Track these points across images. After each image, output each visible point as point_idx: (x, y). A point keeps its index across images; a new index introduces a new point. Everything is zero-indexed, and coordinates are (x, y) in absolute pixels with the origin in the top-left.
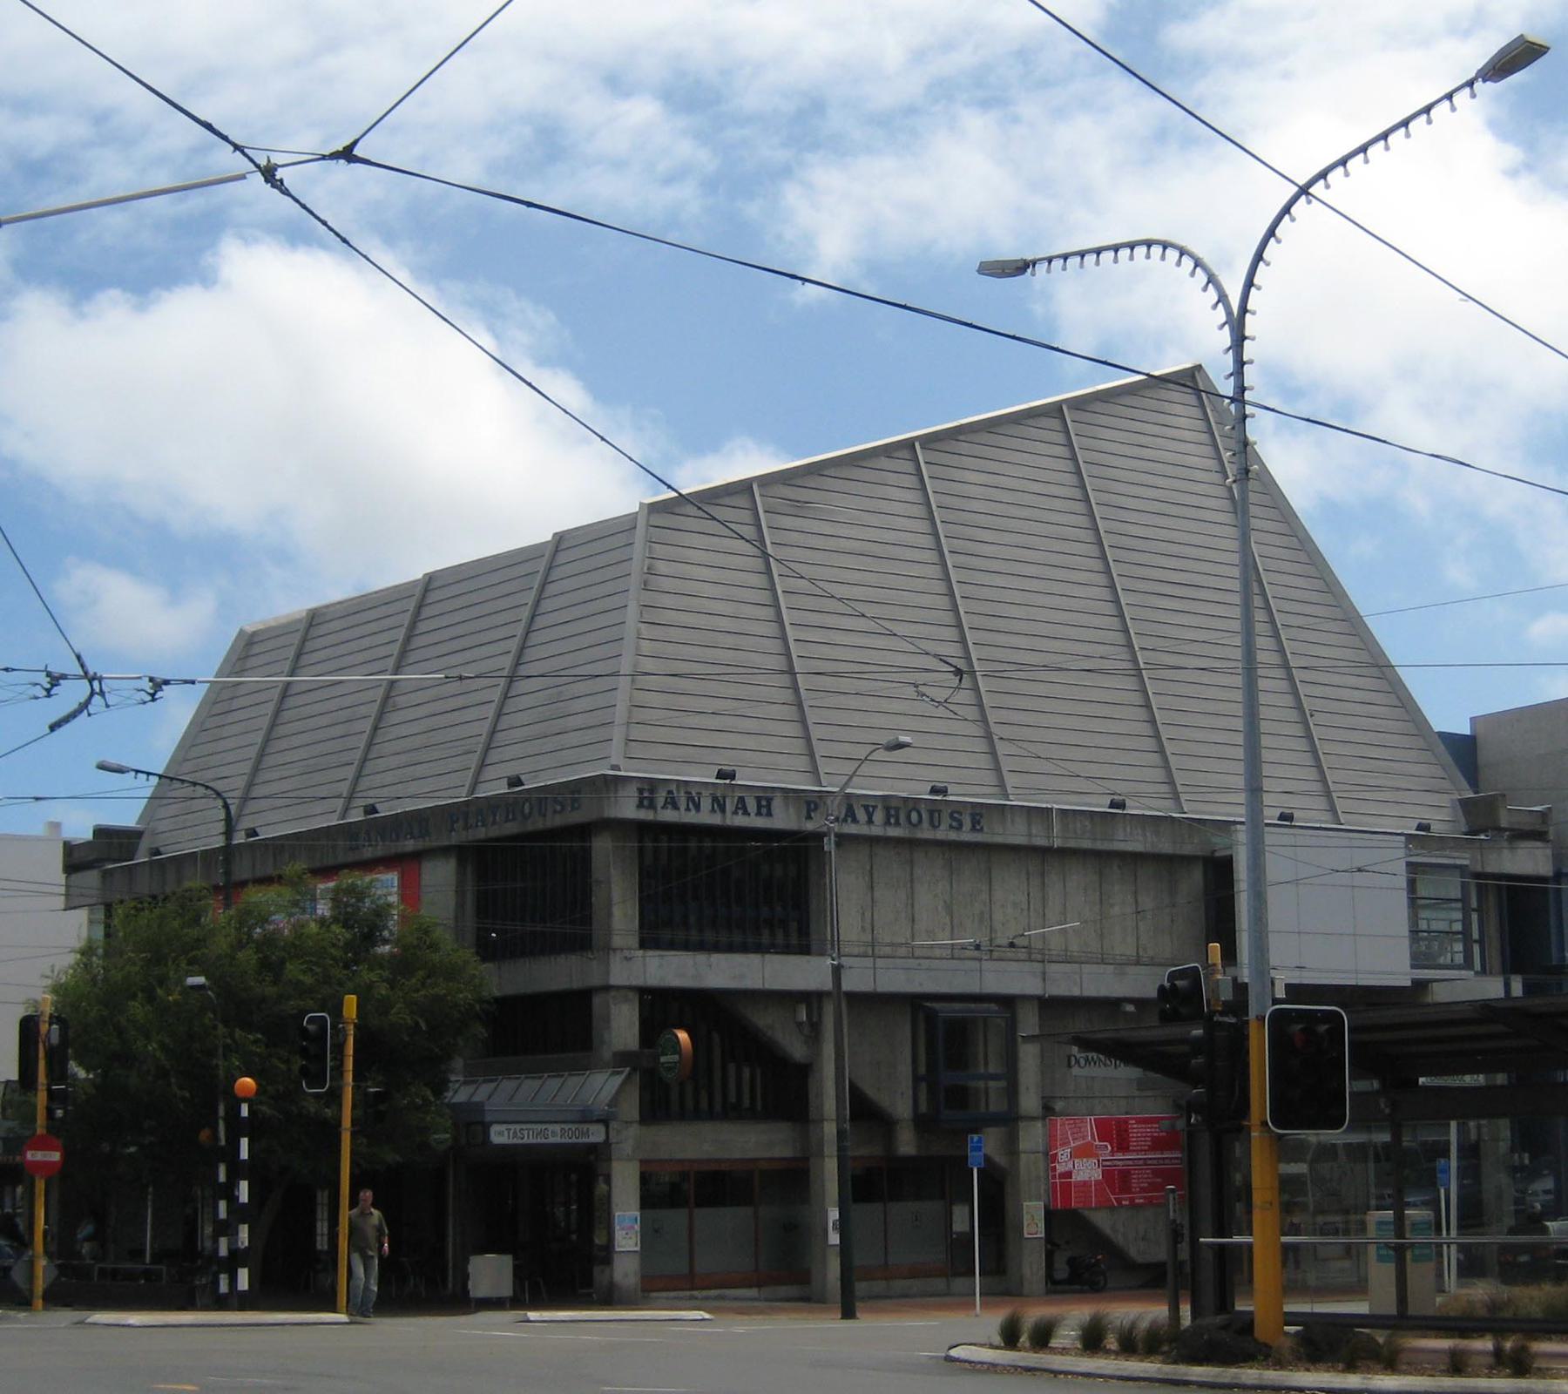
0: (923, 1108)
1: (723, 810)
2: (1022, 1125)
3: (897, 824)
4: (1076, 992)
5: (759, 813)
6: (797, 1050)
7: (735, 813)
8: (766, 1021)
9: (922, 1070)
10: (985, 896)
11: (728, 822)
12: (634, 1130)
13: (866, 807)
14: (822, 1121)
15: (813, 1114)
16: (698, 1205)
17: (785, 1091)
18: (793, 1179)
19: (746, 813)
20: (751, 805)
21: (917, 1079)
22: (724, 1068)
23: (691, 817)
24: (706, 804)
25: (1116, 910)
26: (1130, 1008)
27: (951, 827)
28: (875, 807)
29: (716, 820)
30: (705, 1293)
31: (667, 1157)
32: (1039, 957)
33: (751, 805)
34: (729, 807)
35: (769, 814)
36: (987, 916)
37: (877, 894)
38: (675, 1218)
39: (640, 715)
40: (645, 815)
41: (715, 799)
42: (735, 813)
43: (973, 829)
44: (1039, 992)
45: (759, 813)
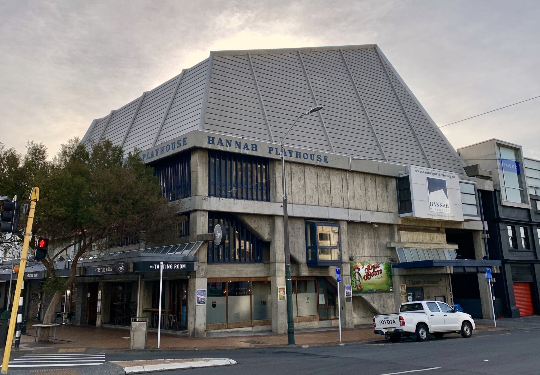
0: (310, 259)
1: (240, 148)
2: (343, 265)
3: (300, 158)
4: (359, 220)
5: (252, 150)
6: (265, 235)
7: (244, 149)
8: (254, 224)
9: (309, 245)
10: (329, 185)
11: (241, 152)
12: (205, 266)
13: (289, 151)
14: (275, 262)
15: (272, 260)
16: (229, 295)
17: (262, 250)
18: (265, 284)
19: (248, 149)
20: (250, 147)
21: (307, 248)
22: (250, 249)
23: (228, 149)
24: (233, 144)
25: (370, 193)
26: (376, 226)
27: (318, 160)
28: (292, 151)
29: (237, 150)
30: (232, 330)
31: (218, 277)
32: (347, 207)
33: (250, 147)
34: (242, 147)
35: (256, 150)
36: (329, 192)
37: (293, 182)
38: (220, 300)
39: (214, 71)
40: (210, 146)
41: (236, 142)
42: (244, 149)
43: (325, 162)
44: (347, 219)
45: (252, 150)
